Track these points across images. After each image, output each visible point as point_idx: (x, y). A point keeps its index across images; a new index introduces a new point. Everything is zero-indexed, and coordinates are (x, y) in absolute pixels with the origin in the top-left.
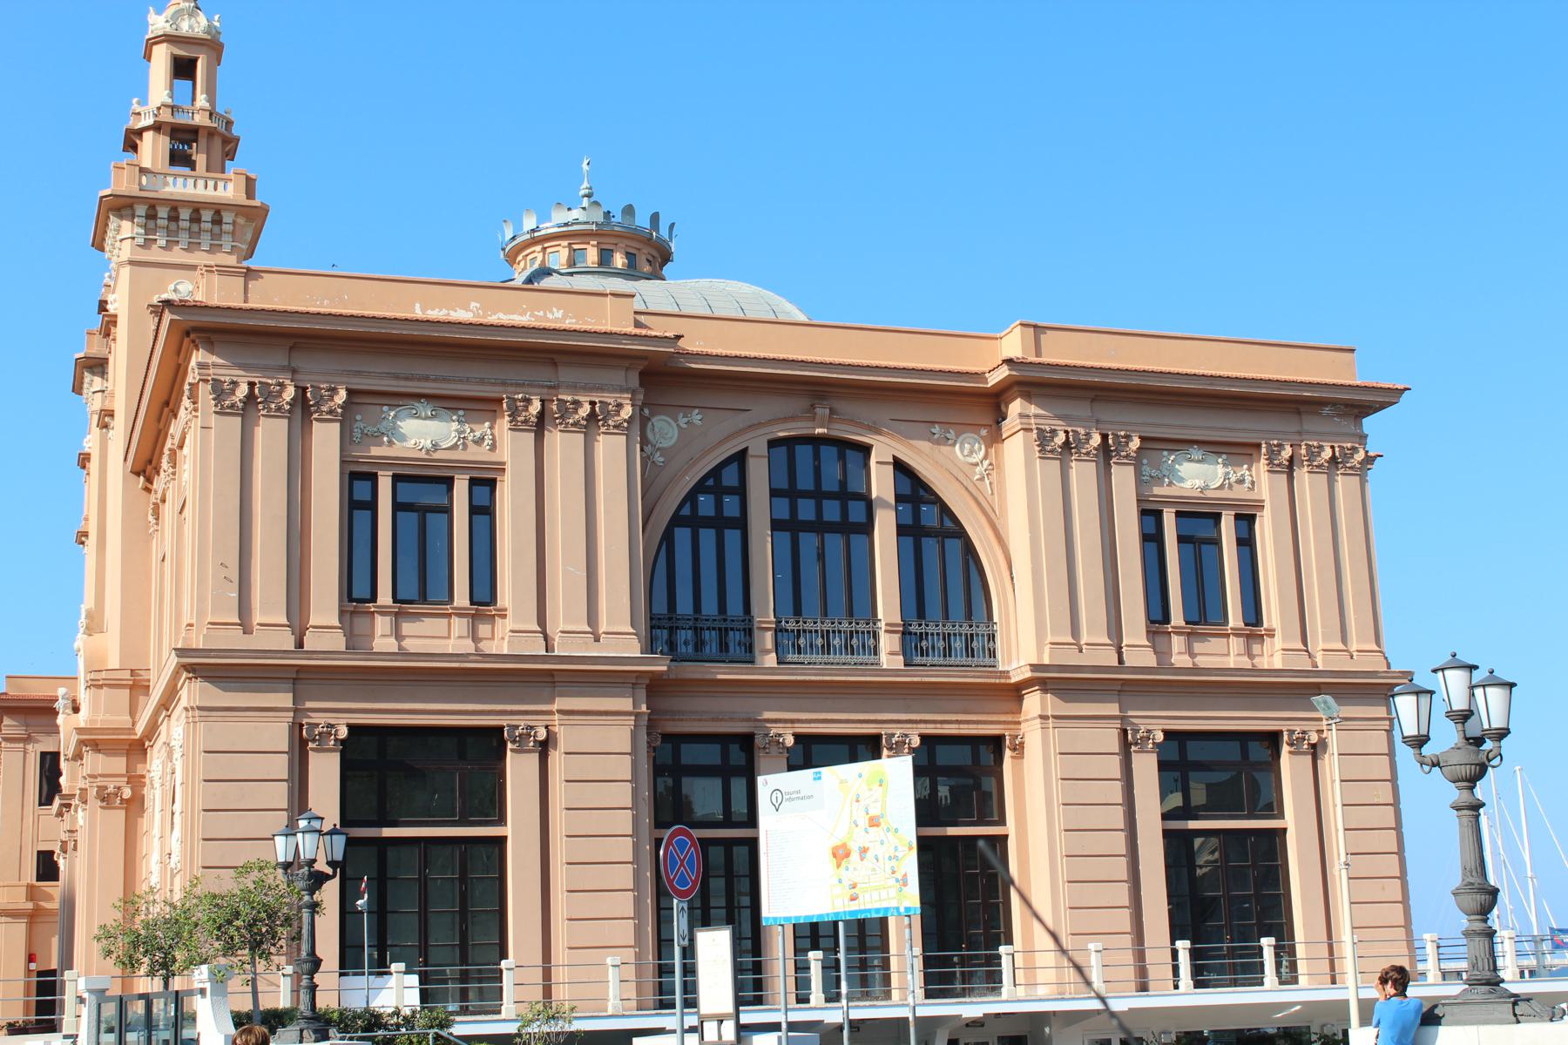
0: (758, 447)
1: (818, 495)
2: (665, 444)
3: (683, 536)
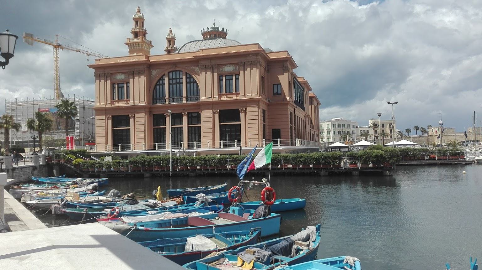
0: (166, 73)
1: (176, 79)
2: (154, 74)
3: (158, 87)
